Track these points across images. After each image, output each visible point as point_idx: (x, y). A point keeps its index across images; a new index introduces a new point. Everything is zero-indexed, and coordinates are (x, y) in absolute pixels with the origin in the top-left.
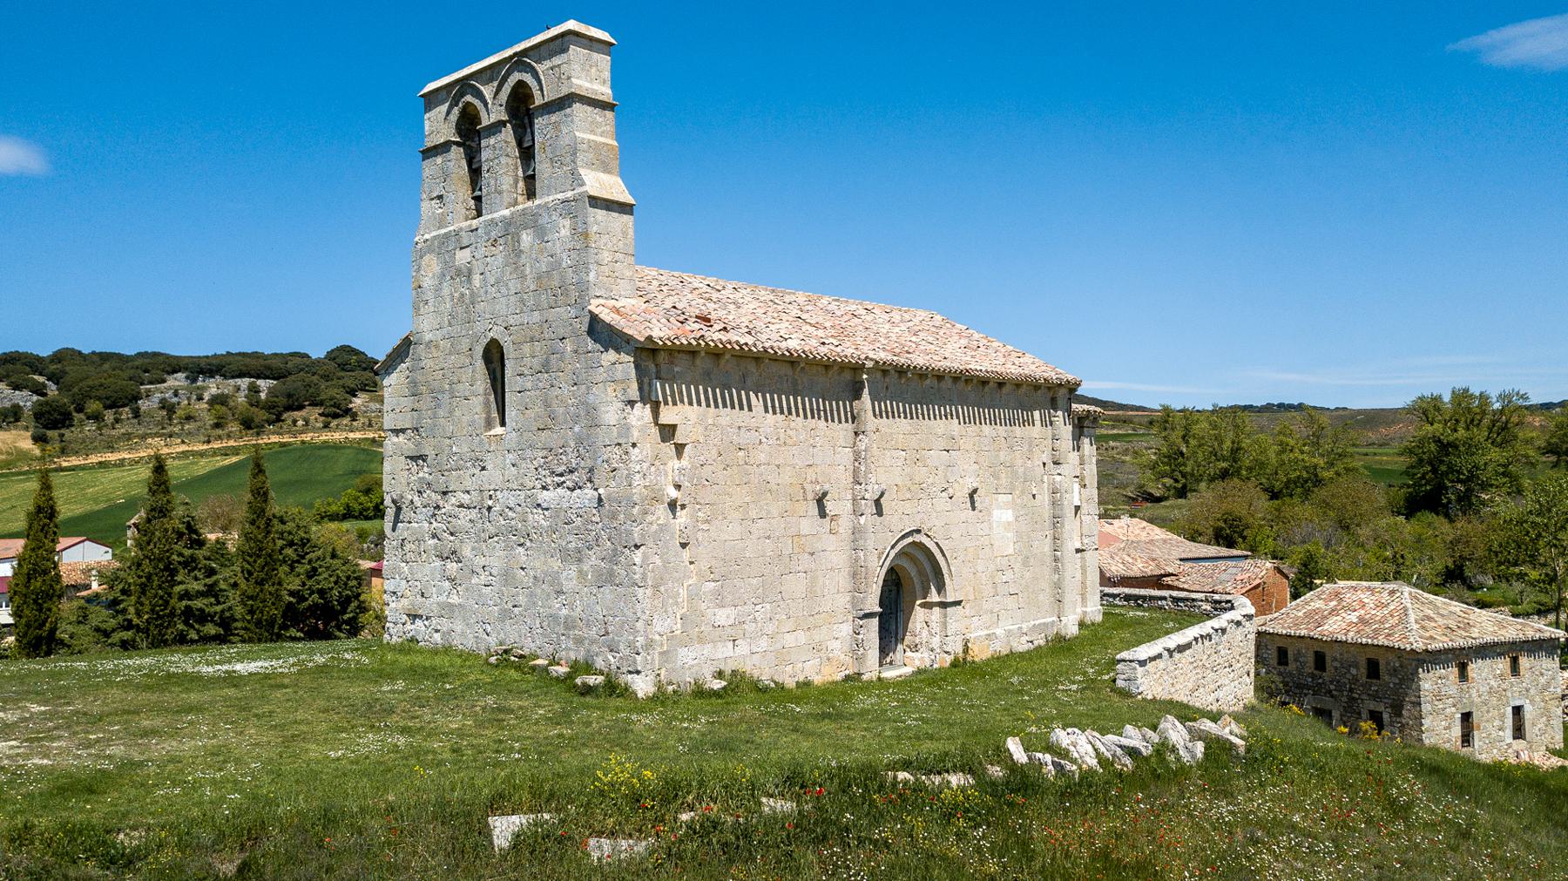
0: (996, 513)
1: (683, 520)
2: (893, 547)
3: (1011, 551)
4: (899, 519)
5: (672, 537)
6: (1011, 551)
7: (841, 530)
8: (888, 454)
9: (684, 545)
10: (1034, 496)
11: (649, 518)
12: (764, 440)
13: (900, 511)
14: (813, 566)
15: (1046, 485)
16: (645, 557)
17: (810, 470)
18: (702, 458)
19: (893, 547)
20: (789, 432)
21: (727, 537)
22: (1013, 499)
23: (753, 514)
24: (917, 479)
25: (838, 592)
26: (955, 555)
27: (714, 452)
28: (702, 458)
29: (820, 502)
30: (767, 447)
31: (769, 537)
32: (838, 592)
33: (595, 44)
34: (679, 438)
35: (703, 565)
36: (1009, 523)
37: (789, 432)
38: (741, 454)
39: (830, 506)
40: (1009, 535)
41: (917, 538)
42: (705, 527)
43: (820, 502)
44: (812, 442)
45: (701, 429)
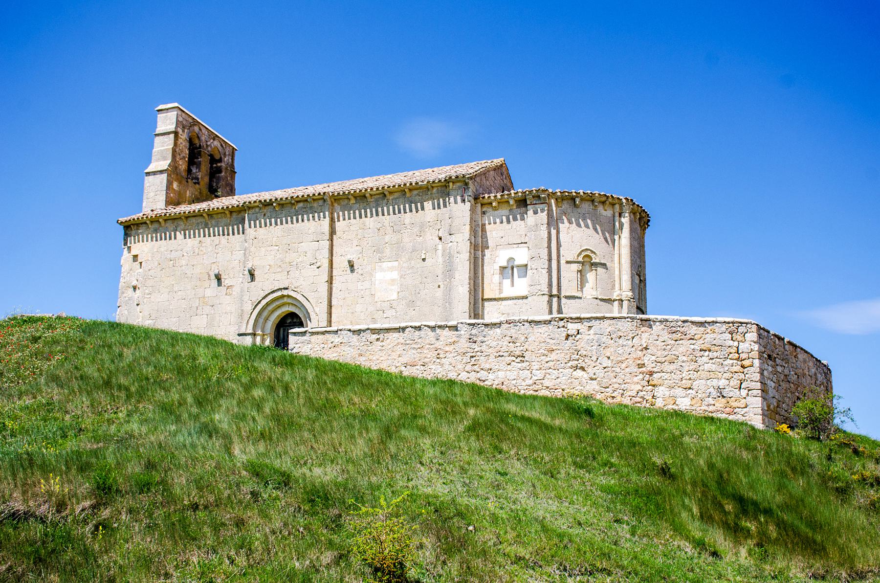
0: (379, 276)
1: (138, 295)
2: (264, 298)
3: (394, 296)
4: (266, 284)
5: (134, 302)
6: (394, 296)
7: (234, 293)
8: (263, 249)
9: (138, 305)
10: (424, 260)
11: (125, 295)
12: (185, 254)
13: (272, 279)
14: (212, 312)
15: (440, 252)
16: (120, 311)
17: (213, 266)
18: (150, 267)
19: (264, 298)
20: (201, 248)
21: (160, 300)
22: (399, 264)
23: (176, 289)
24: (287, 260)
25: (230, 324)
26: (320, 301)
27: (156, 264)
28: (150, 267)
29: (218, 278)
30: (187, 258)
31: (185, 299)
32: (230, 324)
33: (169, 110)
34: (140, 261)
35: (146, 313)
36: (393, 280)
37: (201, 248)
38: (172, 262)
39: (226, 282)
40: (393, 288)
41: (285, 292)
42: (148, 296)
43: (218, 278)
44: (216, 251)
45: (150, 255)
